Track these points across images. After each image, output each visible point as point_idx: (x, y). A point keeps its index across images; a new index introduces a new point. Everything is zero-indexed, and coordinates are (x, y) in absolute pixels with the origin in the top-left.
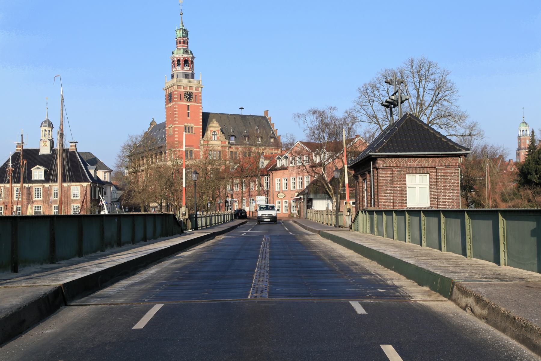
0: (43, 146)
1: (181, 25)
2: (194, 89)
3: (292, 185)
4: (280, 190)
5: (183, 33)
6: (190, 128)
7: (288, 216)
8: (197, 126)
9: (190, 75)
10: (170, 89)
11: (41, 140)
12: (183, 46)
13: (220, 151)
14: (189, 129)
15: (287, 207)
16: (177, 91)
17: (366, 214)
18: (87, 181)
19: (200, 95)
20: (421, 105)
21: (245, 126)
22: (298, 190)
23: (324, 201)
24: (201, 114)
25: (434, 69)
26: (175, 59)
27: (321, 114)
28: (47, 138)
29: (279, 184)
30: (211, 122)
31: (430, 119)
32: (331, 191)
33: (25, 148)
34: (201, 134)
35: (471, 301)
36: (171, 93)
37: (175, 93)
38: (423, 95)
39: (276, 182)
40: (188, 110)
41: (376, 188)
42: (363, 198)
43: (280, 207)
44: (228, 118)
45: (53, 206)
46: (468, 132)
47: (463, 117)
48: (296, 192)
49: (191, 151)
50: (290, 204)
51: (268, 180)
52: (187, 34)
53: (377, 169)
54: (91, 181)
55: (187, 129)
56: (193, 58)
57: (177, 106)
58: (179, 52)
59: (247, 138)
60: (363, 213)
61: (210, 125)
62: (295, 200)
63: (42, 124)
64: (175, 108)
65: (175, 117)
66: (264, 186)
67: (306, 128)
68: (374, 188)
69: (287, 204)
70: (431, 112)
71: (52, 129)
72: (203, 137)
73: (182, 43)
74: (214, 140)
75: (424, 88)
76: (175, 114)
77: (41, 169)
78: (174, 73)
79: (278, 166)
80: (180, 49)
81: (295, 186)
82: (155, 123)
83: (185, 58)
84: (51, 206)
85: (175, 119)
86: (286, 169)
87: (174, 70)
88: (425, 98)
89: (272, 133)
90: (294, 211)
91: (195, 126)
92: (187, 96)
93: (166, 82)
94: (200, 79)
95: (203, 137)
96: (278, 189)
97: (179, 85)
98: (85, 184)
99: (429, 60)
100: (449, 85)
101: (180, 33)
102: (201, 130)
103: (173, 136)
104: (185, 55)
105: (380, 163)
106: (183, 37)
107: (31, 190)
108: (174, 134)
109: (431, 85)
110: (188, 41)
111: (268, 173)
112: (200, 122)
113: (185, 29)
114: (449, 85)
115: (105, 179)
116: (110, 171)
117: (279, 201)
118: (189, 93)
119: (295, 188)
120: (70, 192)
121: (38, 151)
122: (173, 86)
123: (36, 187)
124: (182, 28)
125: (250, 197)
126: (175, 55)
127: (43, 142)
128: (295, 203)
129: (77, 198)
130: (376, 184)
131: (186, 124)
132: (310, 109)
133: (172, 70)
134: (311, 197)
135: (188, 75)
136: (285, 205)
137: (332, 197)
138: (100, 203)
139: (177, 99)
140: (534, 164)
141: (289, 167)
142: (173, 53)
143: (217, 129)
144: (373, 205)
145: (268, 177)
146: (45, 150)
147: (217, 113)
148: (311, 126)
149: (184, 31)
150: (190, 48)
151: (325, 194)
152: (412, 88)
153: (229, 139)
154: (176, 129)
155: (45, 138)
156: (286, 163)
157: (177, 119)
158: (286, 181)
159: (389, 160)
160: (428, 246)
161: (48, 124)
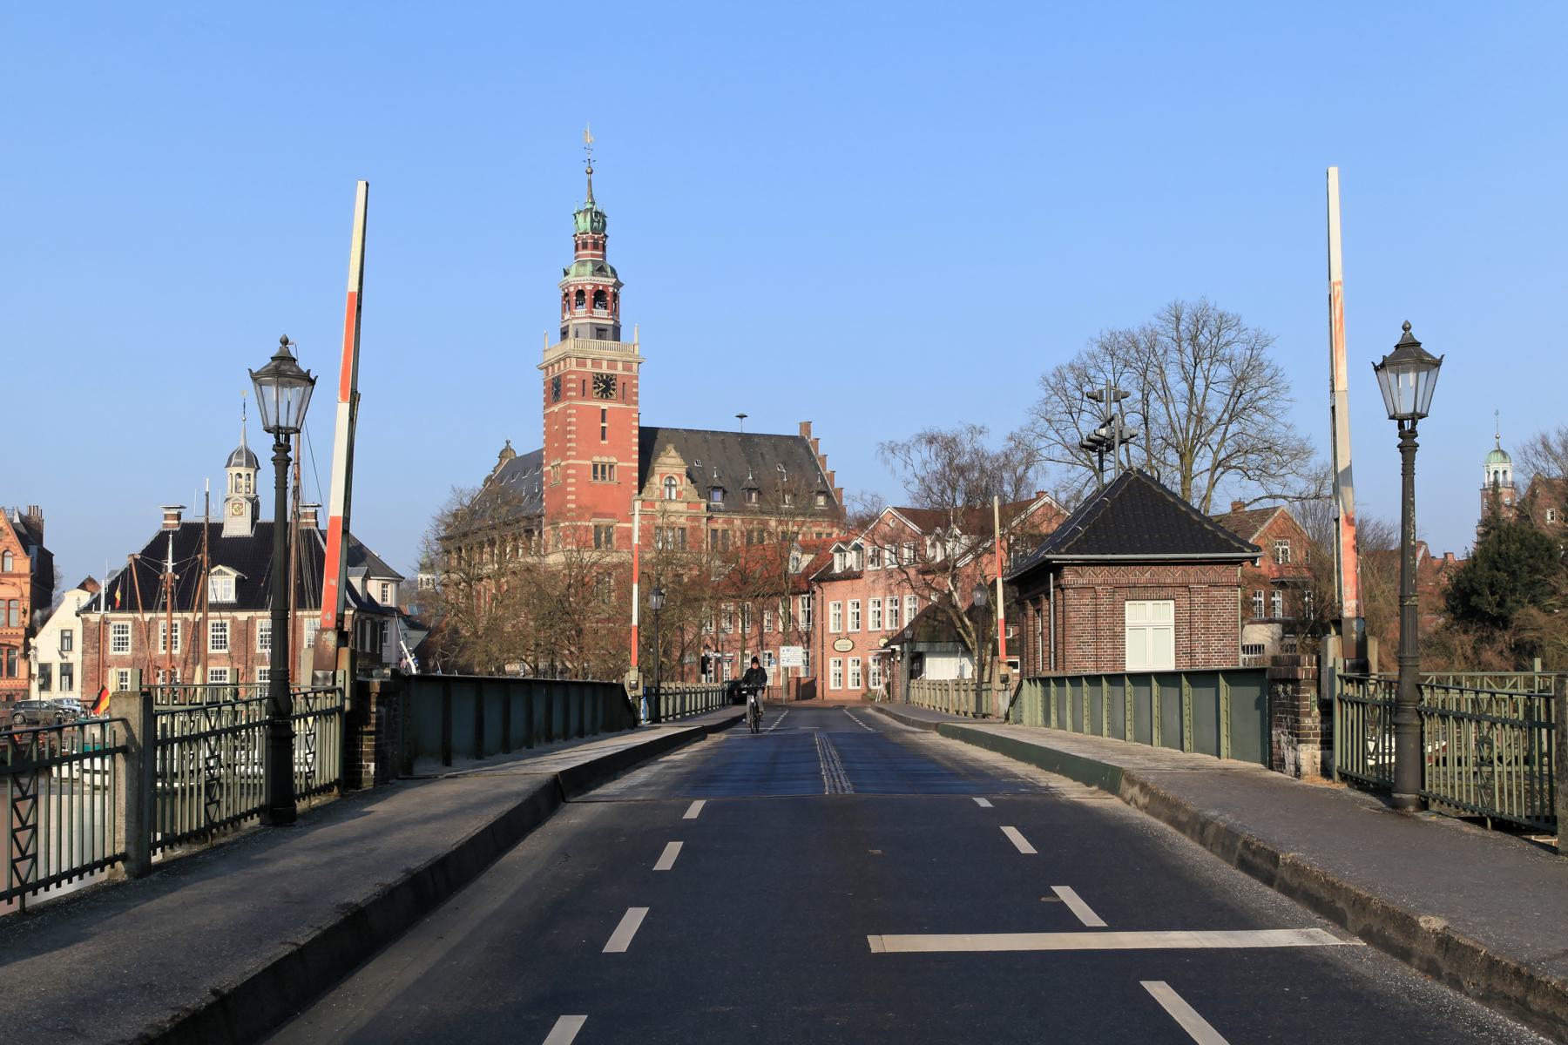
0: (233, 514)
1: (587, 199)
2: (620, 365)
3: (871, 619)
4: (840, 631)
5: (592, 221)
6: (607, 467)
7: (860, 698)
8: (625, 464)
9: (610, 330)
10: (556, 366)
11: (227, 500)
12: (592, 255)
13: (683, 529)
14: (603, 471)
15: (858, 675)
19: (634, 382)
20: (1200, 420)
21: (749, 462)
22: (887, 631)
23: (954, 659)
25: (1233, 333)
26: (572, 289)
27: (948, 445)
28: (243, 494)
29: (839, 615)
30: (662, 453)
31: (1222, 455)
32: (969, 635)
33: (184, 519)
34: (636, 483)
36: (559, 377)
37: (569, 377)
38: (1204, 396)
39: (832, 610)
40: (603, 421)
43: (840, 675)
44: (706, 441)
45: (258, 669)
46: (1313, 488)
48: (882, 637)
49: (609, 527)
50: (866, 667)
52: (605, 224)
54: (356, 606)
55: (600, 470)
56: (618, 285)
57: (574, 411)
58: (582, 270)
59: (754, 495)
61: (659, 460)
62: (879, 657)
64: (570, 416)
65: (570, 441)
66: (800, 620)
67: (911, 479)
69: (859, 667)
70: (1223, 440)
71: (256, 472)
72: (640, 492)
73: (589, 246)
74: (670, 499)
75: (1206, 379)
76: (570, 432)
77: (228, 574)
78: (568, 326)
79: (837, 569)
80: (583, 263)
81: (879, 622)
82: (512, 453)
83: (596, 285)
84: (252, 670)
85: (568, 445)
87: (567, 316)
88: (1208, 405)
90: (875, 684)
91: (620, 464)
92: (601, 385)
93: (547, 348)
94: (636, 341)
95: (640, 492)
97: (581, 355)
99: (1220, 308)
101: (585, 221)
102: (637, 475)
103: (561, 490)
106: (594, 230)
108: (566, 485)
109: (1223, 371)
110: (604, 242)
111: (810, 586)
113: (599, 210)
114: (1268, 372)
115: (383, 600)
116: (398, 579)
117: (838, 659)
118: (607, 377)
119: (879, 626)
120: (302, 634)
121: (220, 527)
122: (564, 359)
124: (592, 209)
125: (762, 649)
126: (570, 278)
128: (879, 664)
131: (597, 459)
132: (921, 431)
133: (563, 318)
134: (921, 650)
136: (852, 668)
137: (974, 649)
138: (404, 660)
139: (574, 394)
140: (1486, 570)
141: (865, 571)
142: (566, 273)
143: (676, 470)
145: (809, 599)
146: (238, 526)
148: (922, 473)
149: (596, 216)
150: (611, 260)
151: (954, 641)
153: (709, 498)
154: (570, 472)
155: (237, 496)
156: (858, 562)
157: (574, 445)
158: (858, 607)
161: (246, 460)
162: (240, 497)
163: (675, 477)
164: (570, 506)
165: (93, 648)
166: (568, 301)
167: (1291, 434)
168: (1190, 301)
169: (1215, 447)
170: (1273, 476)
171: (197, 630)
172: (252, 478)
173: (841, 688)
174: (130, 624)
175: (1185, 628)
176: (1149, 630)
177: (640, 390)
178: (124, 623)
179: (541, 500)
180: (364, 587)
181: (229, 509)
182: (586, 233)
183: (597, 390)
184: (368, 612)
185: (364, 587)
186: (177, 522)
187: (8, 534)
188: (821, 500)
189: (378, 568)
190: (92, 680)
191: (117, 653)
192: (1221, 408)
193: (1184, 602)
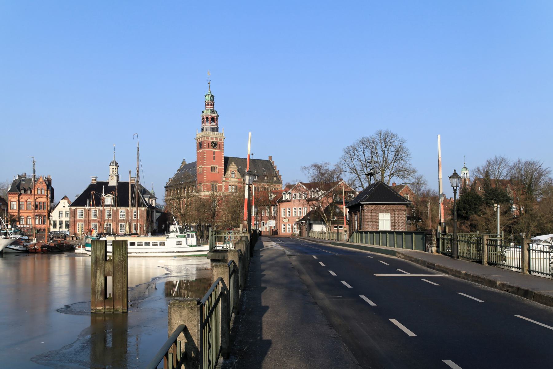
2: (219, 139)
3: (294, 213)
5: (210, 98)
6: (215, 168)
7: (291, 235)
9: (216, 129)
11: (110, 175)
12: (211, 107)
13: (237, 186)
14: (214, 169)
15: (290, 229)
16: (206, 141)
17: (358, 233)
18: (145, 206)
19: (223, 144)
21: (255, 167)
23: (320, 225)
24: (223, 158)
25: (395, 139)
26: (205, 117)
27: (318, 167)
31: (392, 172)
32: (325, 219)
34: (223, 173)
35: (400, 255)
36: (201, 142)
37: (204, 142)
38: (387, 155)
39: (282, 211)
40: (214, 155)
41: (363, 220)
42: (355, 225)
44: (242, 161)
45: (120, 223)
46: (417, 181)
47: (414, 172)
48: (297, 218)
49: (216, 185)
50: (292, 226)
51: (275, 209)
53: (364, 210)
55: (213, 169)
56: (218, 116)
57: (206, 152)
58: (207, 111)
59: (256, 177)
60: (356, 233)
61: (230, 166)
62: (296, 224)
63: (110, 164)
64: (205, 153)
65: (205, 160)
66: (273, 213)
67: (309, 176)
68: (362, 220)
69: (290, 227)
70: (393, 168)
72: (224, 175)
75: (388, 151)
76: (205, 158)
78: (204, 127)
79: (284, 199)
80: (208, 110)
81: (296, 214)
83: (212, 116)
84: (119, 224)
86: (289, 201)
87: (203, 125)
88: (388, 158)
89: (275, 173)
90: (295, 231)
91: (219, 167)
92: (213, 144)
93: (197, 133)
94: (223, 132)
95: (224, 175)
96: (283, 216)
97: (208, 136)
98: (143, 208)
99: (392, 132)
100: (405, 150)
101: (208, 98)
102: (223, 170)
103: (202, 174)
104: (212, 114)
105: (365, 207)
106: (211, 100)
108: (203, 173)
109: (392, 149)
111: (275, 203)
112: (222, 164)
113: (212, 95)
114: (405, 150)
117: (284, 224)
121: (108, 183)
123: (108, 210)
124: (210, 94)
126: (204, 114)
127: (111, 177)
128: (296, 226)
130: (363, 218)
131: (212, 166)
132: (312, 164)
133: (202, 125)
134: (312, 222)
135: (214, 129)
136: (288, 227)
139: (206, 147)
143: (235, 169)
144: (361, 229)
145: (275, 207)
146: (113, 183)
147: (234, 158)
151: (321, 220)
152: (380, 150)
154: (205, 169)
155: (113, 174)
156: (290, 197)
157: (206, 161)
159: (370, 206)
160: (389, 246)
162: (114, 175)
163: (234, 171)
164: (205, 179)
165: (73, 217)
166: (204, 121)
167: (411, 167)
168: (384, 130)
169: (390, 169)
170: (406, 177)
171: (102, 212)
172: (117, 169)
173: (285, 232)
174: (83, 210)
175: (393, 221)
176: (385, 220)
177: (224, 146)
178: (82, 210)
179: (196, 177)
180: (149, 201)
181: (110, 178)
182: (209, 101)
183: (212, 146)
185: (149, 201)
186: (95, 181)
187: (43, 183)
188: (275, 179)
189: (152, 196)
190: (73, 226)
191: (80, 218)
192: (392, 159)
193: (393, 214)
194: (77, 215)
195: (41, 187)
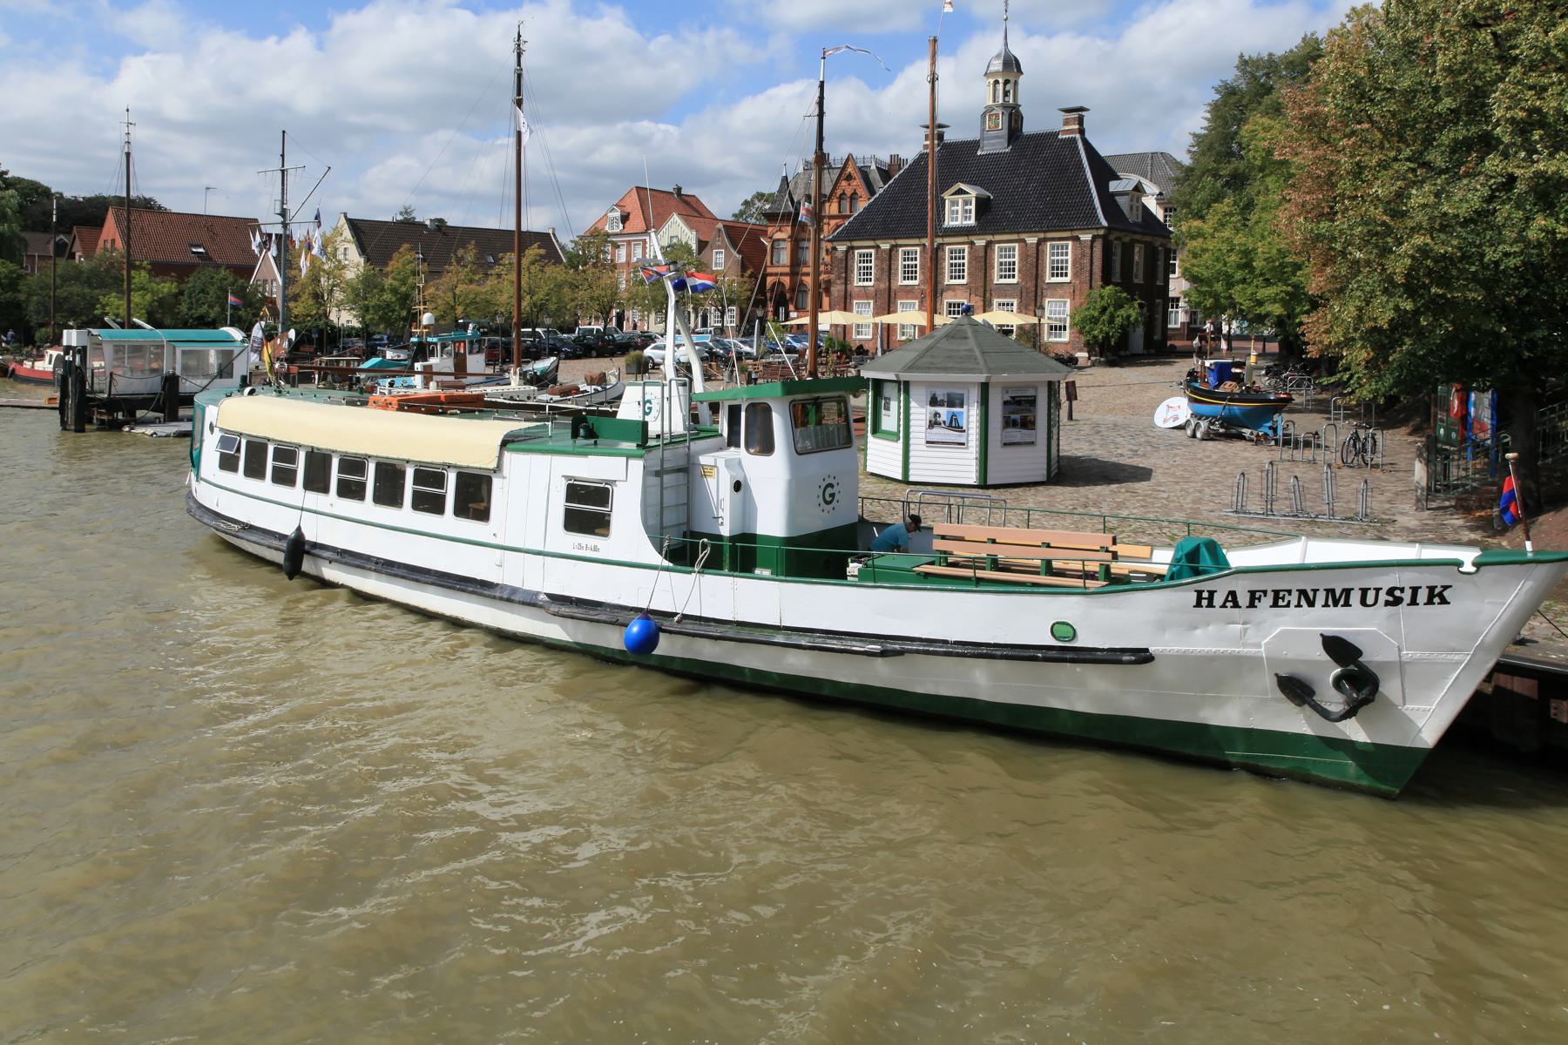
107: (940, 253)
129: (1064, 279)
184: (1134, 232)
194: (852, 271)
195: (849, 192)
